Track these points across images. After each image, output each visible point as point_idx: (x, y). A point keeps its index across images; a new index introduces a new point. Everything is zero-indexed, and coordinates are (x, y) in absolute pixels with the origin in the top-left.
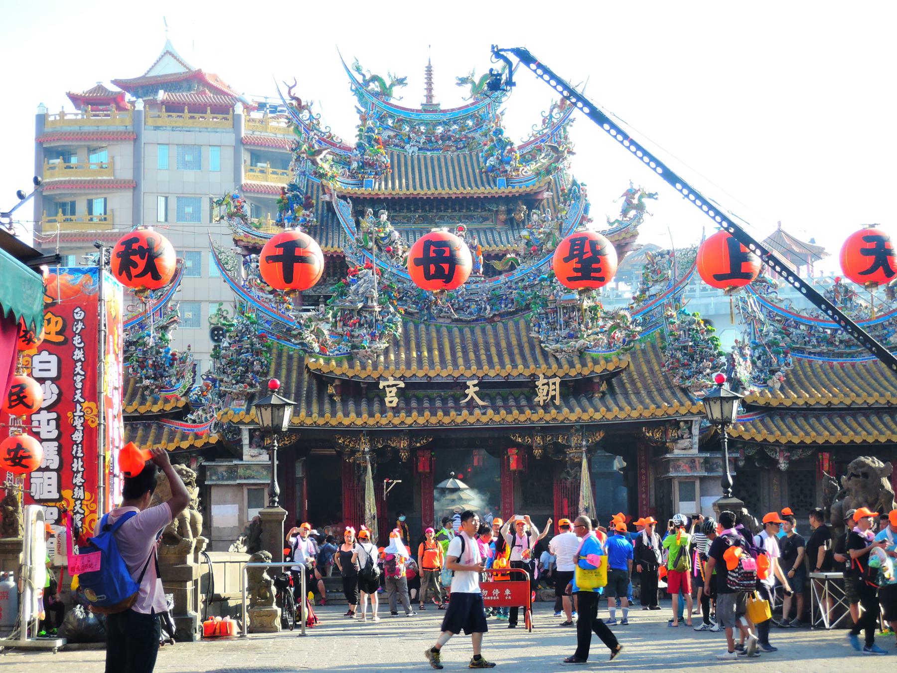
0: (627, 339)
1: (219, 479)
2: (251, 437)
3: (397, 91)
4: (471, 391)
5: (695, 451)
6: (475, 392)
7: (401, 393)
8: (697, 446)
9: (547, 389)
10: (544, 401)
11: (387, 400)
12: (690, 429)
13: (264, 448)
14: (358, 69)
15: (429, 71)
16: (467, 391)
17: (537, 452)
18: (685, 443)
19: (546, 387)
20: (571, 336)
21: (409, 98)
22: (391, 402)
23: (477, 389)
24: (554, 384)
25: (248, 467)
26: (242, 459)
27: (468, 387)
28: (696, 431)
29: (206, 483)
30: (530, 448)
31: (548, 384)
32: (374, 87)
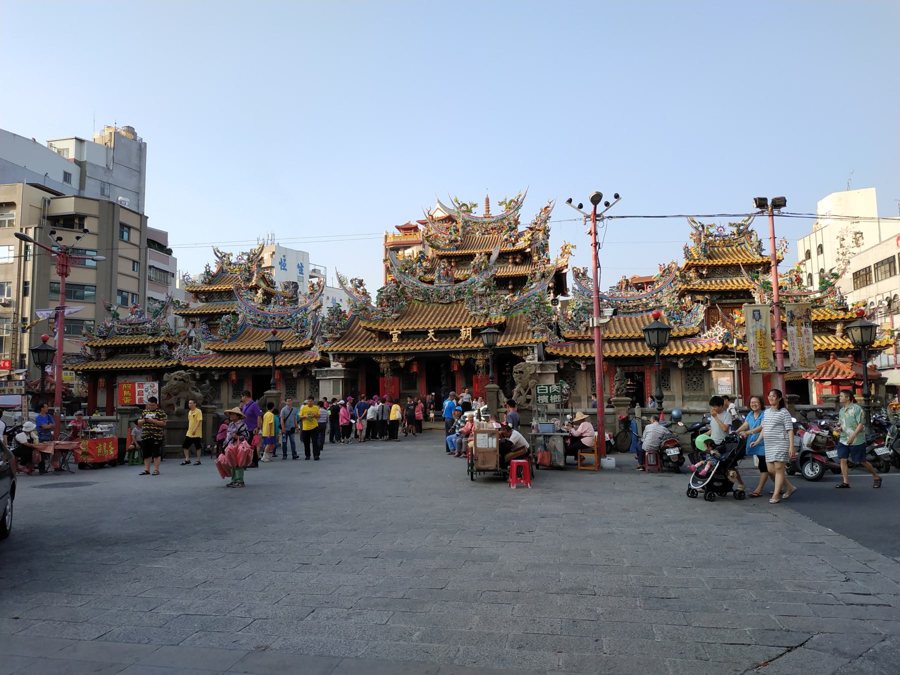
2: (334, 357)
3: (473, 209)
4: (431, 335)
5: (536, 361)
7: (399, 336)
9: (466, 333)
14: (457, 201)
15: (487, 200)
17: (462, 362)
18: (530, 357)
20: (482, 308)
21: (479, 212)
25: (332, 371)
30: (459, 360)
32: (464, 208)
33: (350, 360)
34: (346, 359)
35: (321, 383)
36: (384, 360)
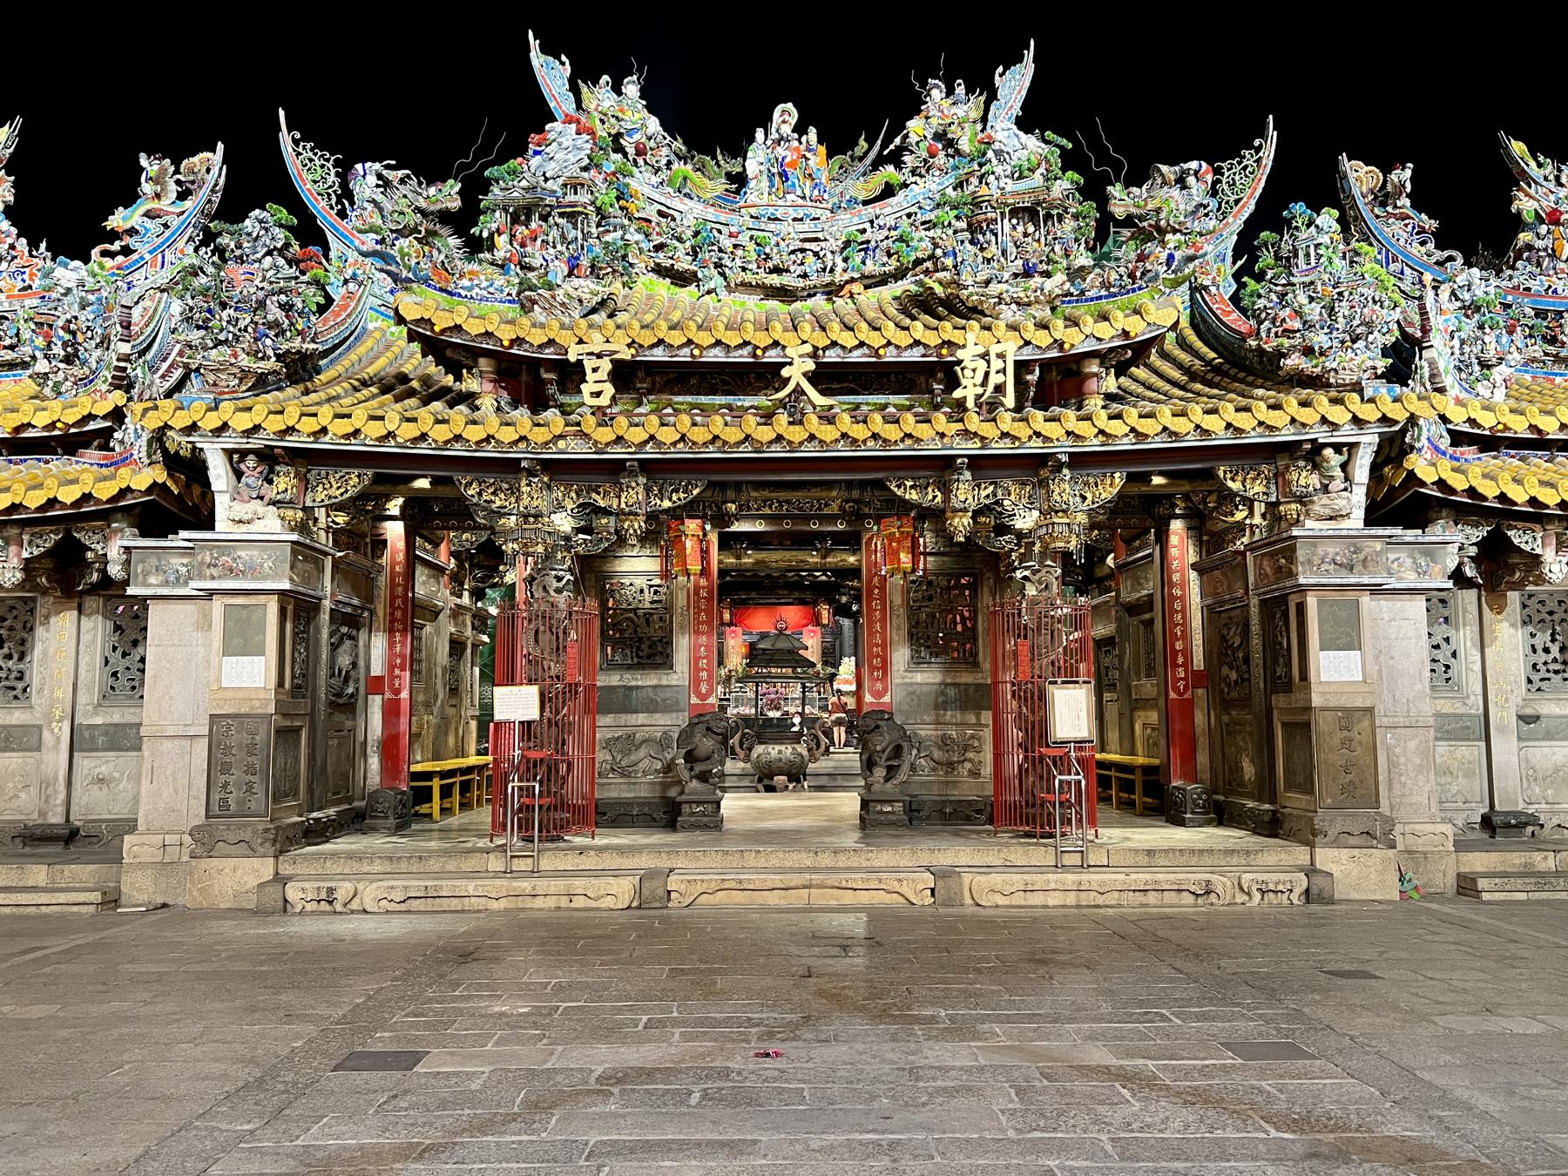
0: (1178, 255)
1: (166, 583)
5: (1356, 521)
6: (804, 374)
8: (1359, 514)
10: (979, 397)
13: (274, 503)
16: (785, 372)
22: (598, 394)
24: (1001, 356)
26: (211, 526)
28: (1361, 473)
29: (130, 591)
35: (154, 610)
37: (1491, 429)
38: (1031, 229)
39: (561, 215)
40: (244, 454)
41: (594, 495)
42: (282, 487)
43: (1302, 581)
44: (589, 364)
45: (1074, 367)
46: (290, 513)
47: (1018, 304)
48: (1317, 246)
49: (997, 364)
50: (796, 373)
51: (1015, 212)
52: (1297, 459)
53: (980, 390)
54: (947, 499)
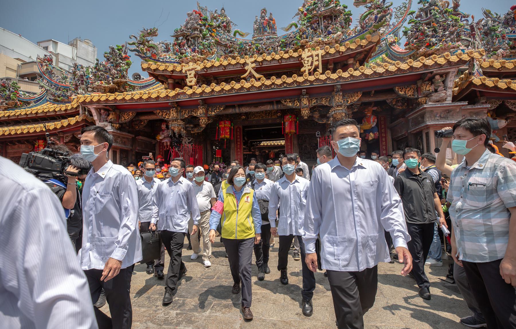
8: (450, 99)
10: (309, 70)
11: (188, 80)
12: (444, 82)
16: (246, 68)
17: (305, 113)
19: (311, 59)
22: (191, 82)
23: (254, 65)
24: (317, 55)
27: (248, 64)
31: (312, 56)
33: (126, 118)
34: (119, 117)
36: (173, 114)
37: (498, 69)
38: (330, 22)
39: (191, 38)
40: (100, 109)
41: (193, 113)
42: (111, 117)
43: (428, 123)
44: (188, 73)
45: (345, 62)
46: (115, 125)
47: (326, 44)
48: (430, 10)
49: (316, 58)
50: (250, 68)
51: (325, 17)
52: (426, 81)
53: (310, 67)
54: (300, 105)
